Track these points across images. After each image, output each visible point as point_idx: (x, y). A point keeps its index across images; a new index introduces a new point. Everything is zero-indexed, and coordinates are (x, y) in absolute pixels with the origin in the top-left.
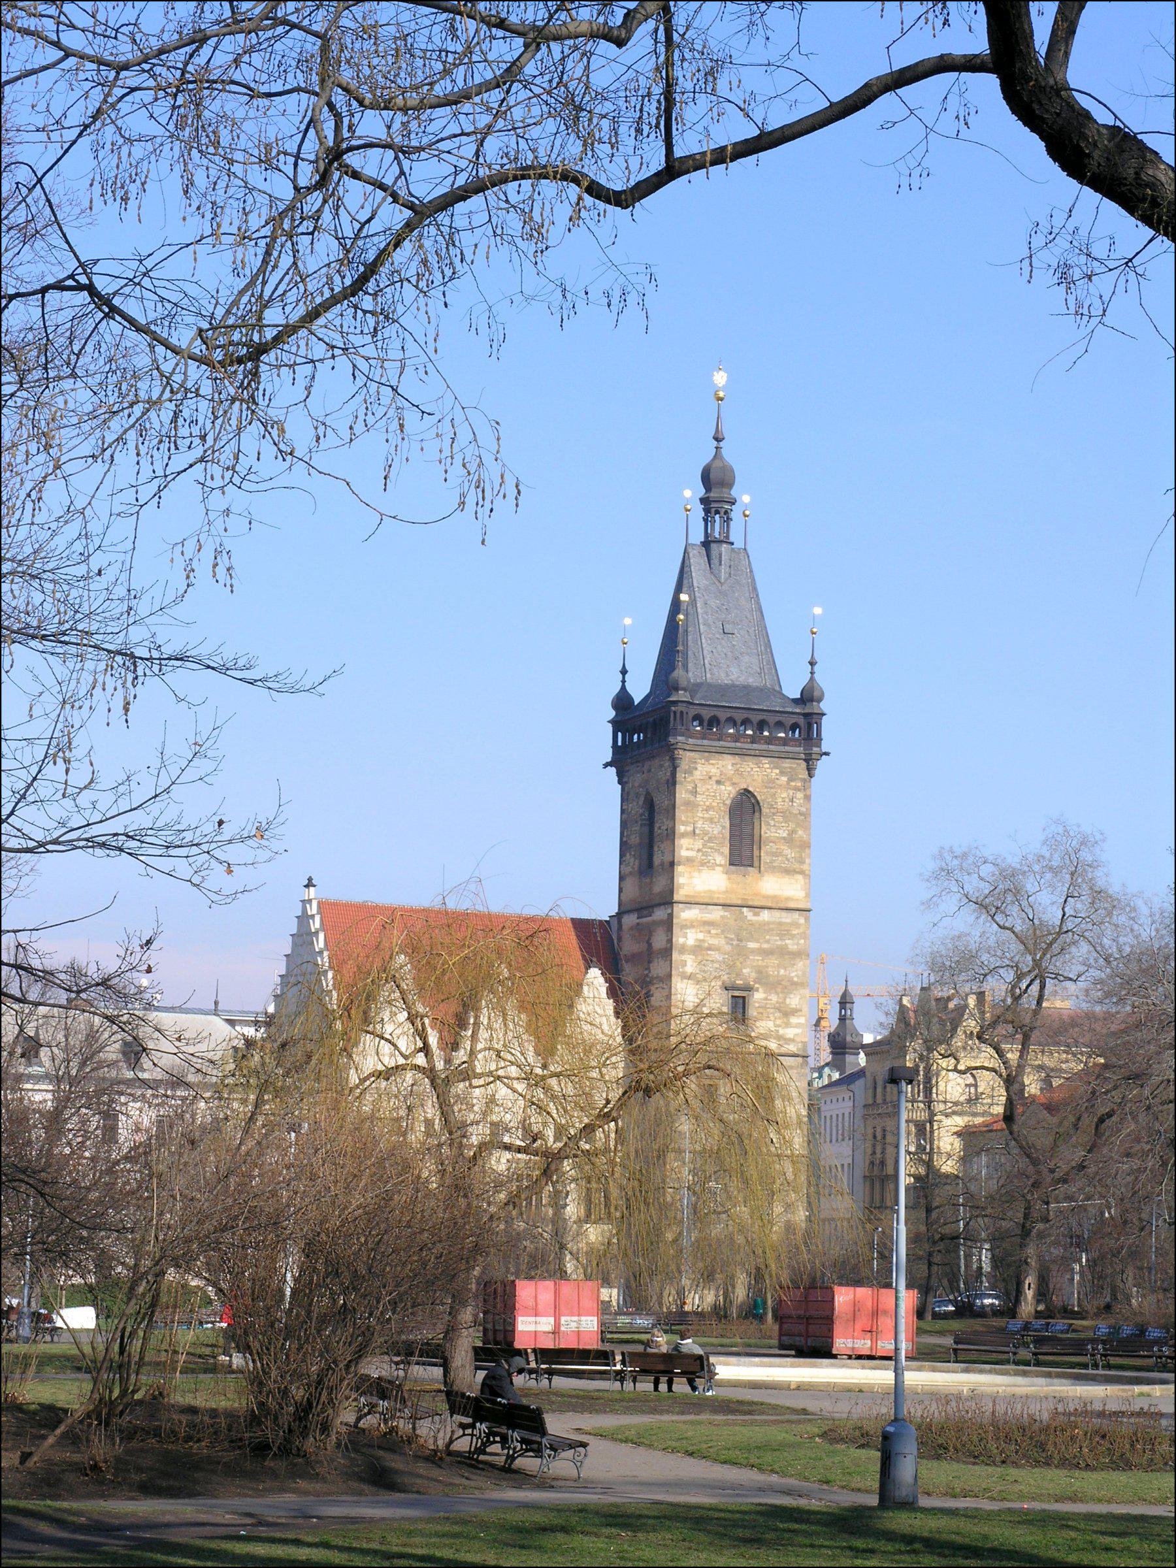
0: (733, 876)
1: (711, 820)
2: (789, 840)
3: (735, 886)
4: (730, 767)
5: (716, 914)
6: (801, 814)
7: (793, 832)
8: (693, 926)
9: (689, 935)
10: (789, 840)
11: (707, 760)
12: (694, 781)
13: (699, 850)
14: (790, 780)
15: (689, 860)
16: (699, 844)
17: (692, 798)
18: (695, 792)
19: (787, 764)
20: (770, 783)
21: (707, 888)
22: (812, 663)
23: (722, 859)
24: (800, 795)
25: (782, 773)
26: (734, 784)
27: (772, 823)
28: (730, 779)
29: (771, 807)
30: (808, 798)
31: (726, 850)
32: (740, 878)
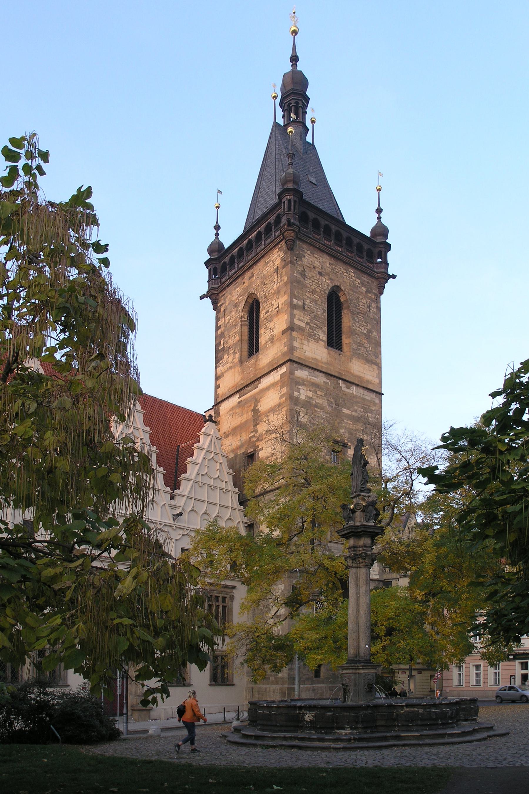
0: (331, 352)
1: (316, 301)
2: (368, 336)
3: (333, 360)
4: (328, 265)
5: (321, 379)
6: (375, 320)
7: (370, 331)
8: (305, 385)
9: (302, 391)
10: (368, 336)
11: (313, 254)
12: (302, 266)
13: (307, 324)
14: (367, 291)
15: (301, 329)
16: (307, 319)
17: (302, 279)
18: (303, 274)
19: (365, 278)
20: (354, 288)
21: (314, 356)
22: (379, 211)
23: (323, 336)
24: (373, 305)
25: (362, 284)
26: (330, 279)
27: (357, 320)
28: (328, 274)
29: (356, 307)
30: (379, 309)
31: (326, 329)
32: (337, 356)
